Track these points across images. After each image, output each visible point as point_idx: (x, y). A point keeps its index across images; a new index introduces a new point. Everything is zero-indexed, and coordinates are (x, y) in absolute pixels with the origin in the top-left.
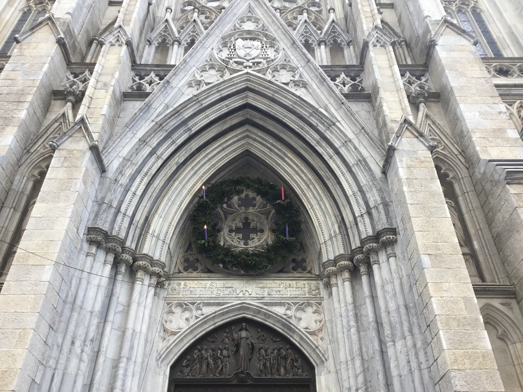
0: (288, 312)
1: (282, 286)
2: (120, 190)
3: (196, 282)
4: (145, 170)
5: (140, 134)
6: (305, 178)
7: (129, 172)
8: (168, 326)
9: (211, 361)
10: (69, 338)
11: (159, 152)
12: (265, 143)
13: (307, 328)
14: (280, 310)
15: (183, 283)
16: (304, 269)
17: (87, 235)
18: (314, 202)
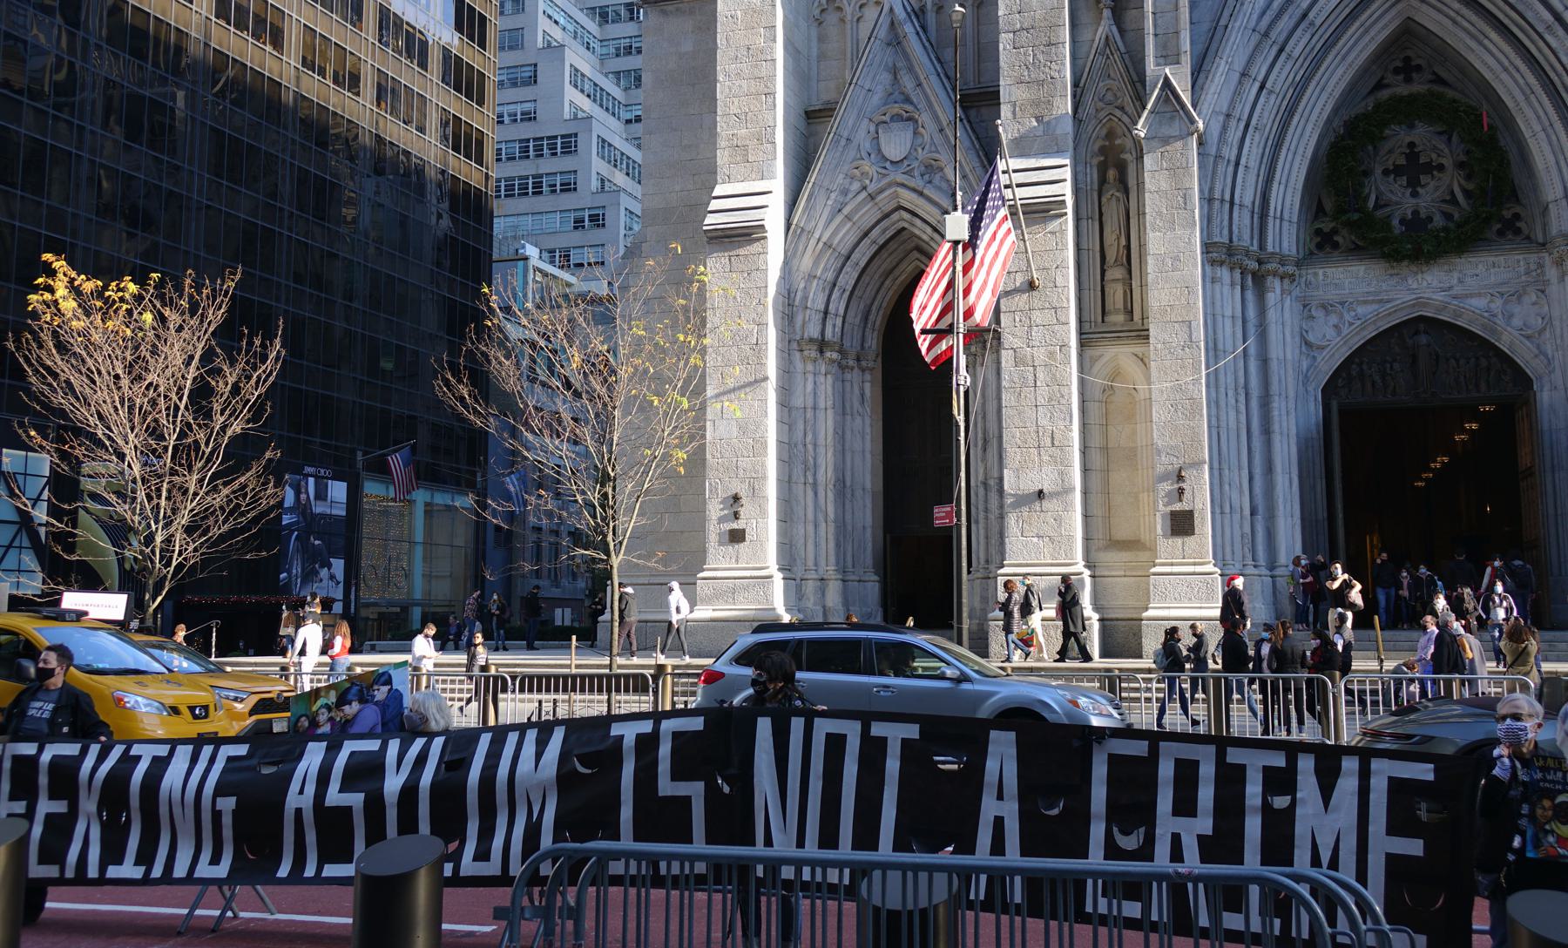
0: (1493, 306)
1: (1480, 266)
2: (1231, 169)
3: (1341, 269)
4: (1254, 122)
5: (1239, 66)
6: (1521, 81)
7: (1234, 135)
8: (1311, 338)
9: (1377, 378)
10: (1222, 390)
11: (1268, 85)
12: (1445, 8)
13: (1521, 329)
14: (1478, 303)
15: (1321, 272)
16: (1518, 231)
17: (1207, 253)
18: (1537, 128)
